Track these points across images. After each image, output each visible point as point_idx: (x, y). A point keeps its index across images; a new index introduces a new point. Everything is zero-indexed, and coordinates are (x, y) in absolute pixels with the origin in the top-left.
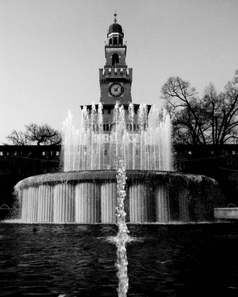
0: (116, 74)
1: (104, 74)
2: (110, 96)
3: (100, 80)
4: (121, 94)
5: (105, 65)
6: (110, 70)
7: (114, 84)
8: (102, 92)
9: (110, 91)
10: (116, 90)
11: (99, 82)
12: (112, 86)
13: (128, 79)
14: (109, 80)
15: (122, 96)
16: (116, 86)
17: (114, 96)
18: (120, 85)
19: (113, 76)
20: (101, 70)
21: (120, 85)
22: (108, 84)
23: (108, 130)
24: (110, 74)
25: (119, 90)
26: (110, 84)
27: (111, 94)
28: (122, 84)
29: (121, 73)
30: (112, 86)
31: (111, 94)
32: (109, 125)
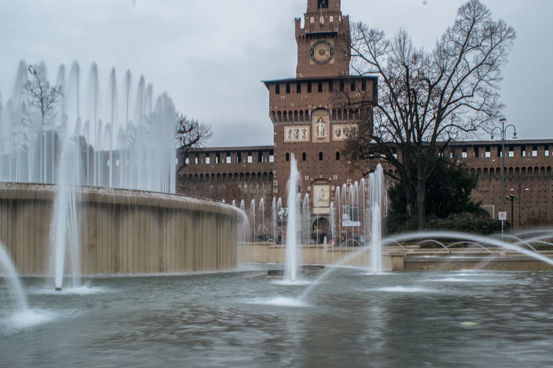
0: (321, 26)
1: (302, 26)
2: (312, 63)
3: (296, 38)
4: (330, 59)
5: (305, 12)
6: (312, 20)
7: (319, 43)
8: (299, 58)
9: (312, 55)
10: (322, 53)
11: (295, 40)
12: (315, 45)
13: (342, 33)
14: (310, 36)
15: (332, 62)
16: (323, 47)
17: (318, 62)
18: (329, 44)
19: (317, 30)
20: (298, 21)
21: (329, 44)
22: (309, 44)
23: (307, 119)
24: (312, 26)
25: (328, 53)
26: (312, 43)
27: (314, 60)
28: (331, 42)
29: (332, 25)
30: (315, 45)
31: (314, 60)
32: (310, 112)
